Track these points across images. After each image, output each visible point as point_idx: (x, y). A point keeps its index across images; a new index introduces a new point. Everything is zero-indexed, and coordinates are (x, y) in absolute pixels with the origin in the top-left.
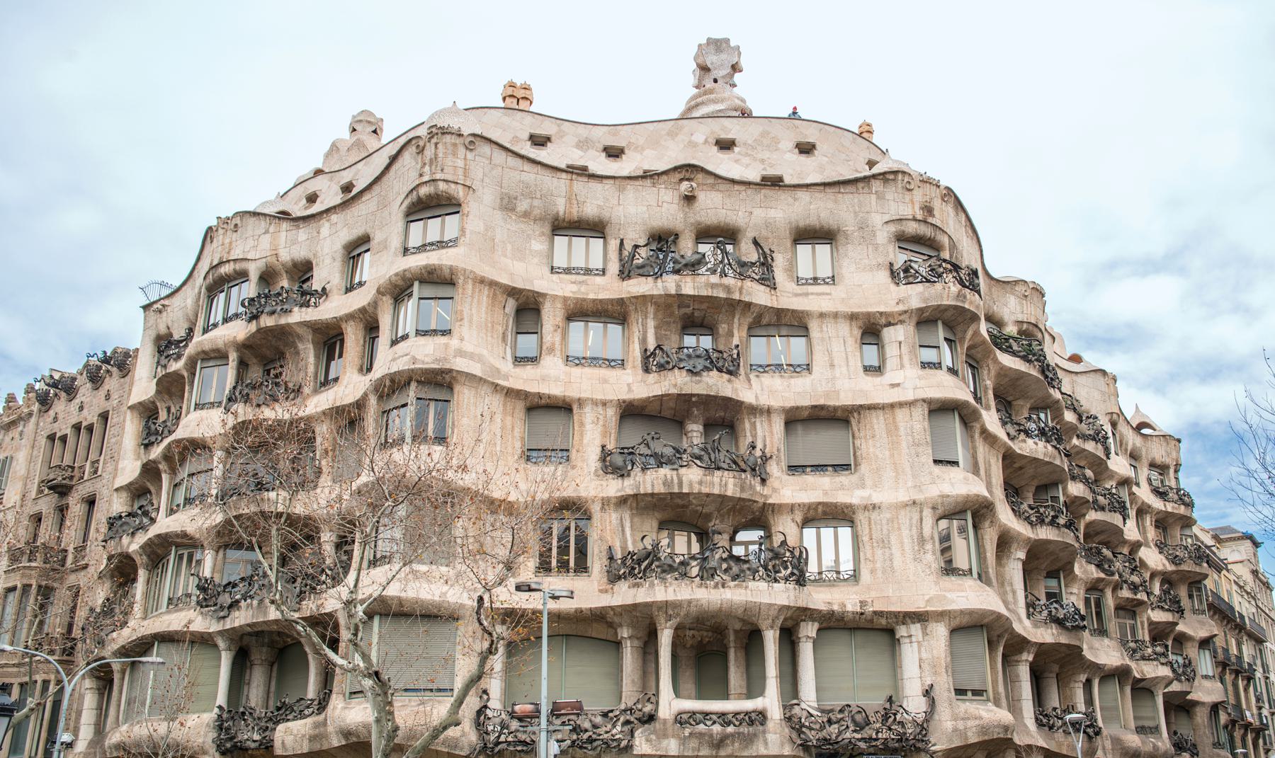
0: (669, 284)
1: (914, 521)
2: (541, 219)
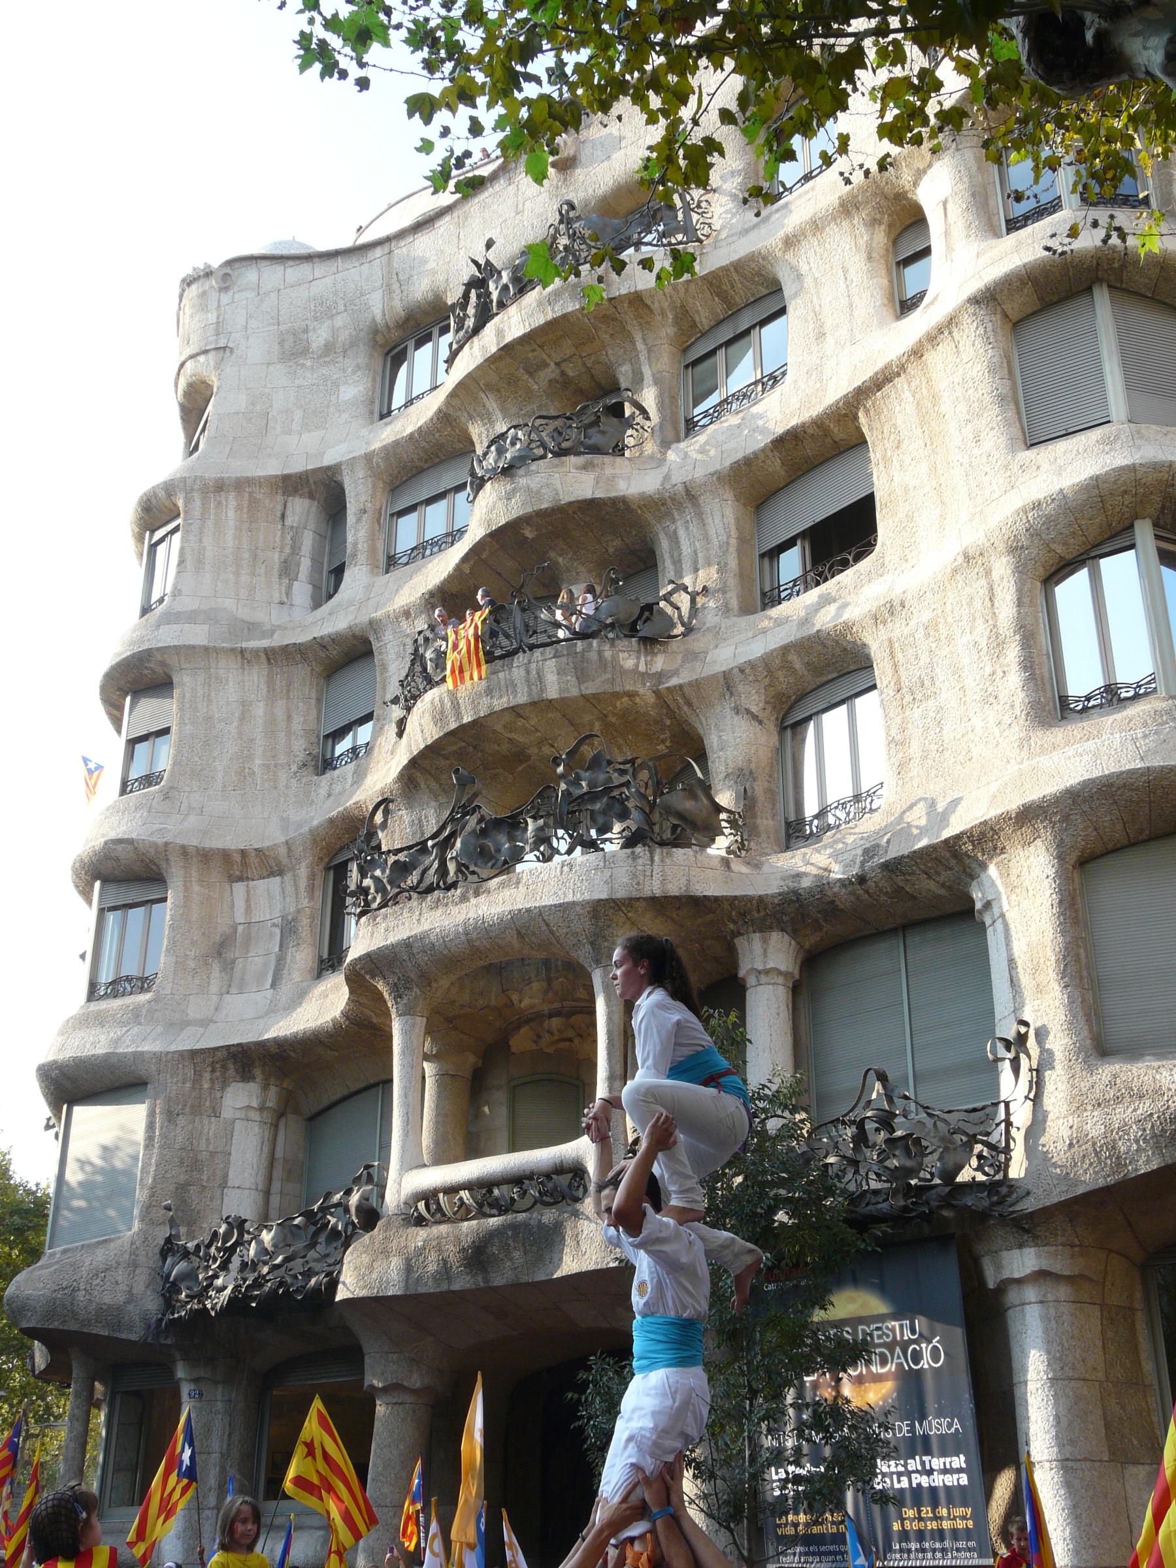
0: (488, 341)
1: (978, 604)
2: (353, 344)
